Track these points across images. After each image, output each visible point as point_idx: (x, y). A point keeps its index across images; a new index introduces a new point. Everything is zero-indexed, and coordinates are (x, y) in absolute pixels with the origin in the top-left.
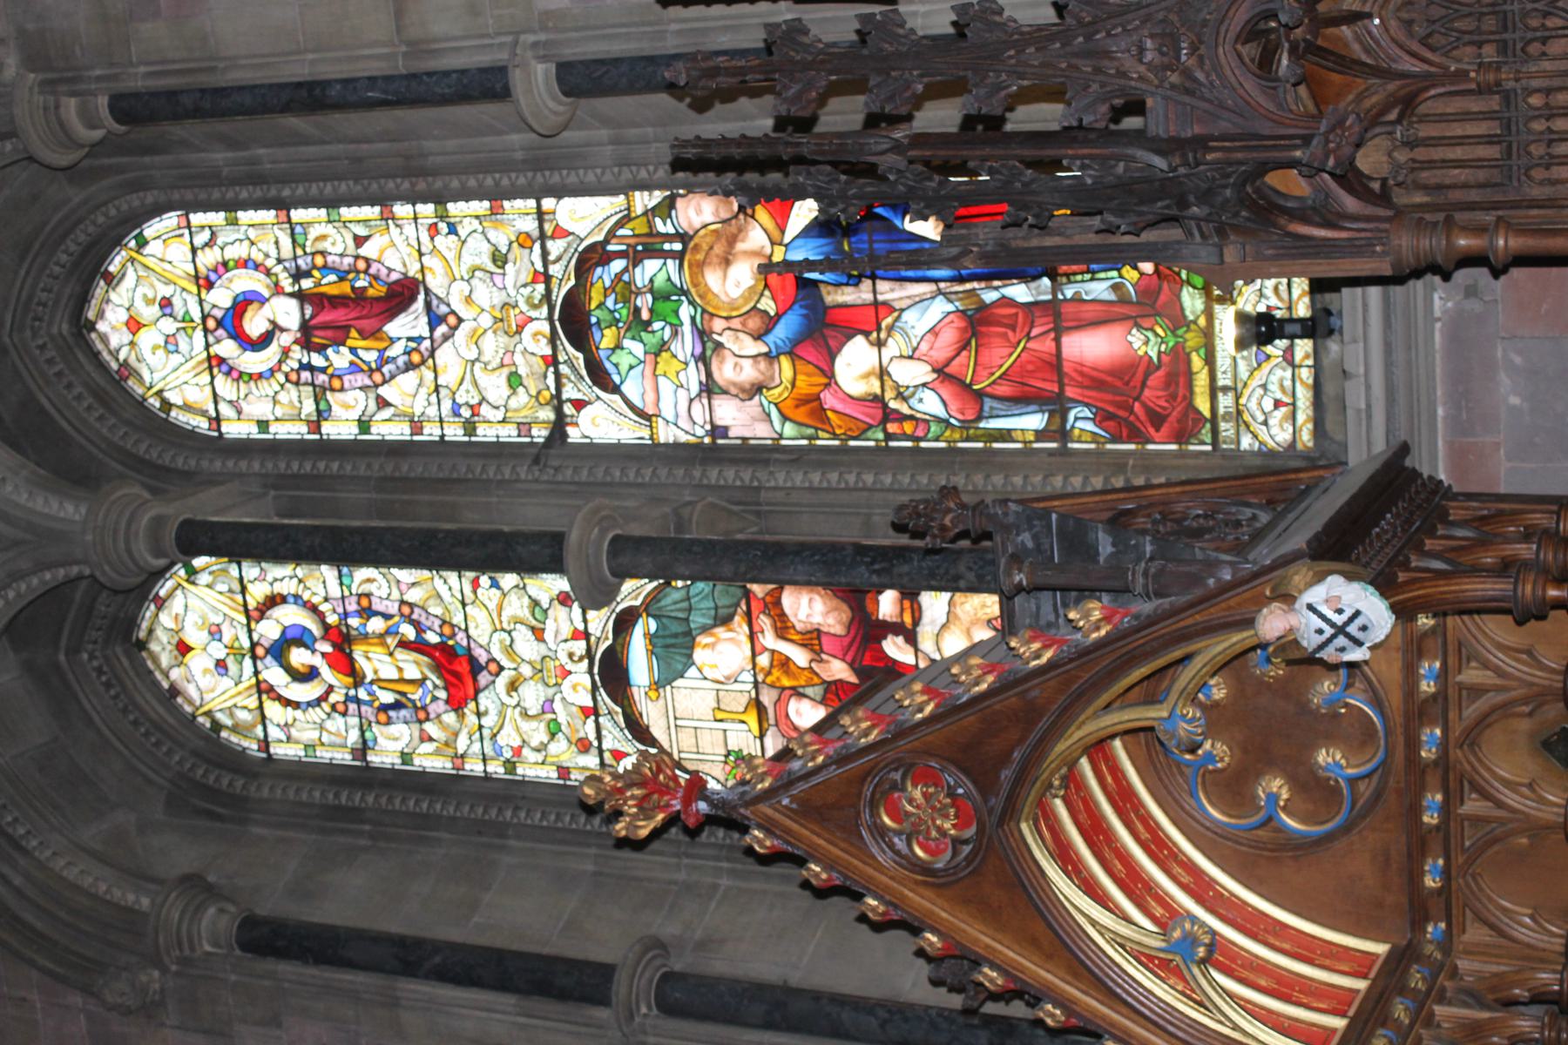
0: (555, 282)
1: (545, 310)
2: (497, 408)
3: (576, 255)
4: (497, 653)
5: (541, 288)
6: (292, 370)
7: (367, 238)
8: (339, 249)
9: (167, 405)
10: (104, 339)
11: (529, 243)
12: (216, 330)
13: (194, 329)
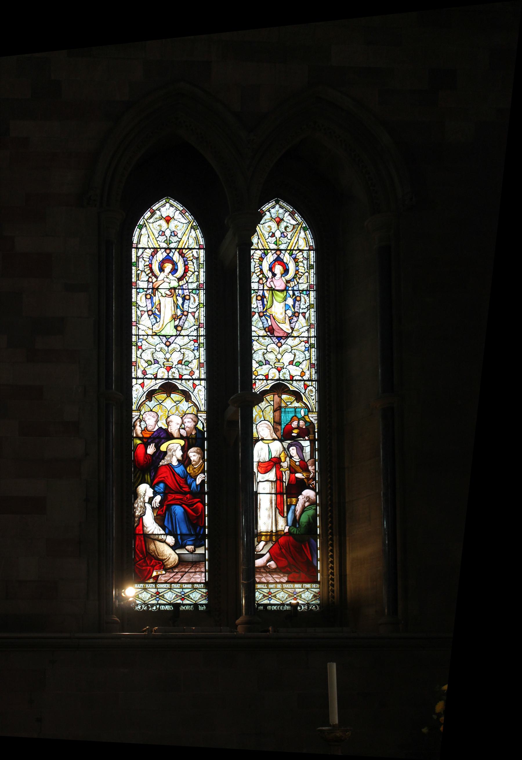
0: (180, 382)
1: (171, 377)
2: (141, 356)
8: (191, 306)
11: (191, 375)
13: (167, 244)
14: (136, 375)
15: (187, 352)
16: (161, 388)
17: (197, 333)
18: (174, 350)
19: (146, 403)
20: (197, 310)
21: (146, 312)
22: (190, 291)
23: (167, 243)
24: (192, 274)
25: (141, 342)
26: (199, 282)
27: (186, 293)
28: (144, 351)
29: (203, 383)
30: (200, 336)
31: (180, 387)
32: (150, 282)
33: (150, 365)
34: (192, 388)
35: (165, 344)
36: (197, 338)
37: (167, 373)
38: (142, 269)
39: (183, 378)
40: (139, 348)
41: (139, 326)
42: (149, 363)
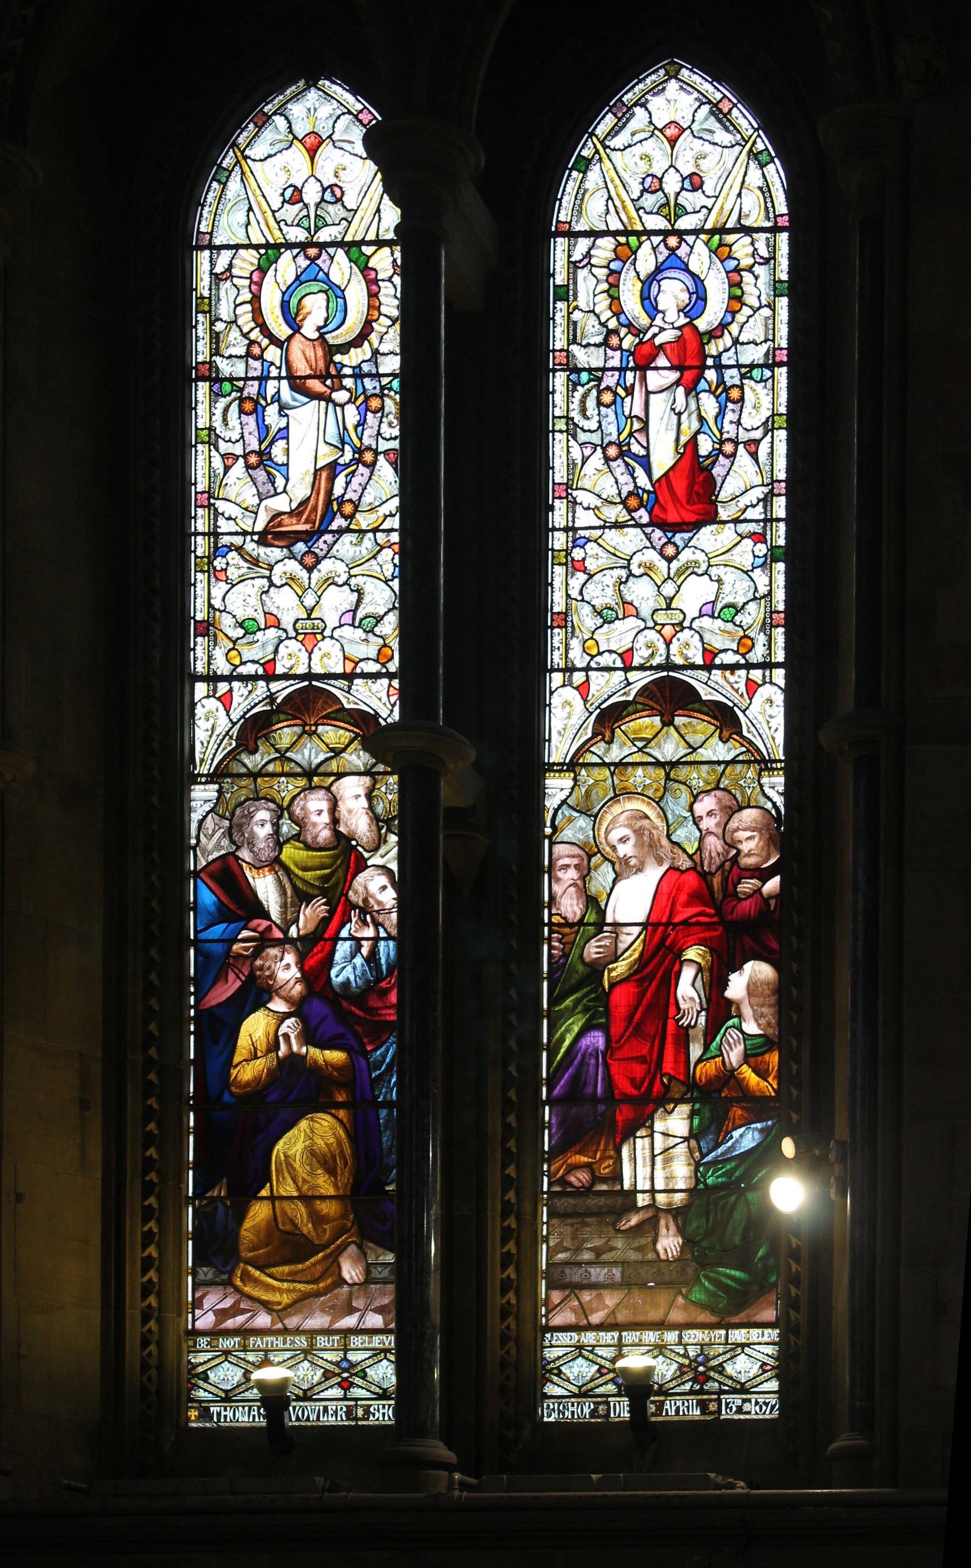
0: (703, 675)
2: (581, 593)
3: (731, 704)
4: (326, 566)
5: (699, 661)
6: (621, 340)
7: (754, 456)
9: (584, 165)
10: (657, 90)
12: (666, 246)
14: (566, 657)
15: (729, 576)
16: (641, 700)
17: (765, 513)
18: (690, 569)
19: (592, 749)
20: (765, 435)
21: (599, 448)
22: (743, 370)
23: (670, 214)
24: (751, 316)
25: (583, 547)
26: (773, 341)
27: (732, 377)
28: (591, 576)
29: (779, 676)
30: (772, 520)
31: (706, 694)
32: (614, 350)
33: (610, 622)
34: (742, 695)
35: (661, 554)
36: (765, 528)
37: (664, 646)
38: (588, 305)
39: (717, 661)
40: (578, 567)
41: (575, 493)
42: (606, 616)
